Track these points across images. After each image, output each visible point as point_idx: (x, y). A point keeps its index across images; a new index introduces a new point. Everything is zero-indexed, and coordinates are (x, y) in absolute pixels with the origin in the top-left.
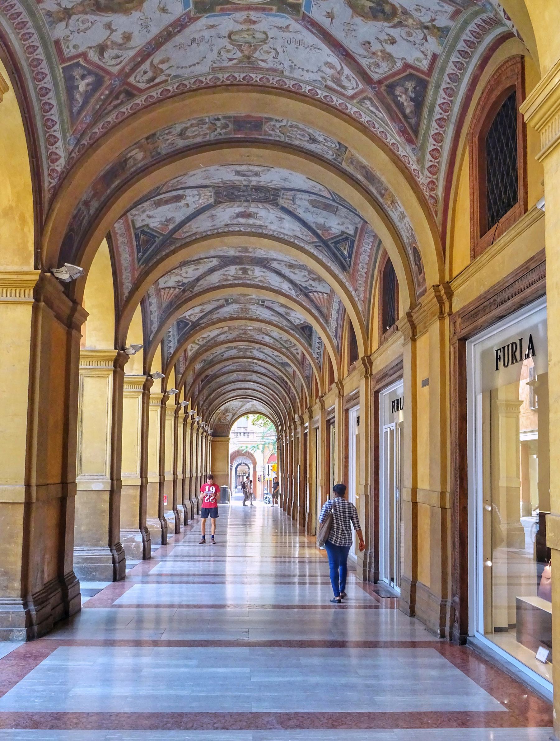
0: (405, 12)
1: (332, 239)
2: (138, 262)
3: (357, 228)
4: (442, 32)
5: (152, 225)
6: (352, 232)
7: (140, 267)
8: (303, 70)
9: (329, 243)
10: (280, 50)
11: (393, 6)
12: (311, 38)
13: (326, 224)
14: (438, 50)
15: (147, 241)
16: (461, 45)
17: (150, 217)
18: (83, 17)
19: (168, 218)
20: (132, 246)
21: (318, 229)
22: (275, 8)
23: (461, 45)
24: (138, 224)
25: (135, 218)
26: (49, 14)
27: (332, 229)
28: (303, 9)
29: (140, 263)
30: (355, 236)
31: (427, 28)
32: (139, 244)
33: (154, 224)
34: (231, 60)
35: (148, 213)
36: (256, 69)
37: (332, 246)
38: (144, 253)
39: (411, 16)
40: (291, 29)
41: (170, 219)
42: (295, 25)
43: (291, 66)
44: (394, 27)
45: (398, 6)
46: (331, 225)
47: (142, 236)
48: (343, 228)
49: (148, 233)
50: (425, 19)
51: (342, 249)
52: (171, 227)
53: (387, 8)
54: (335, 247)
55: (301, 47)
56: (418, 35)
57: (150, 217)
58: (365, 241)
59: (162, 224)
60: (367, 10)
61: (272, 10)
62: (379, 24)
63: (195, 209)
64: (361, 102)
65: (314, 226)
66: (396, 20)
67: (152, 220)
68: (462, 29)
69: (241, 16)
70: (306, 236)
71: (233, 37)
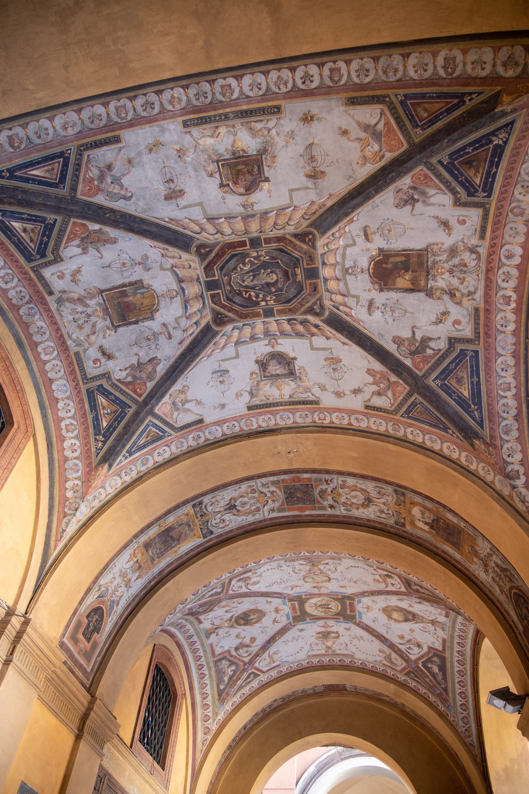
0: (232, 626)
1: (62, 232)
2: (512, 123)
3: (51, 293)
4: (208, 634)
5: (447, 199)
6: (47, 273)
7: (514, 111)
8: (272, 569)
9: (59, 219)
10: (292, 574)
11: (241, 625)
12: (276, 589)
13: (96, 253)
14: (202, 626)
15: (469, 163)
16: (195, 638)
17: (445, 224)
18: (425, 616)
19: (409, 208)
20: (511, 169)
21: (100, 231)
22: (304, 597)
23: (195, 638)
24: (474, 215)
25: (474, 241)
26: (443, 629)
27: (79, 251)
28: (287, 601)
29: (509, 119)
30: (36, 270)
31: (216, 629)
32: (490, 167)
33: (440, 201)
34: (327, 564)
35: (448, 241)
36: (306, 559)
37: (51, 217)
38: (487, 139)
39: (228, 627)
40: (290, 588)
41: (406, 202)
42: (288, 591)
43: (281, 567)
44: (232, 617)
45: (238, 627)
46: (86, 258)
47: (477, 181)
48: (67, 267)
49: (462, 184)
50: (220, 632)
51: (29, 226)
52: (406, 181)
53: (242, 622)
54: (42, 220)
55: (279, 581)
56: (217, 622)
57: (445, 224)
58: (16, 279)
59: (423, 194)
60: (251, 614)
61: (305, 595)
62: (240, 612)
63: (352, 221)
64: (223, 585)
65: (112, 232)
66: (233, 620)
67: (444, 215)
68: (203, 645)
69: (323, 591)
70: (102, 177)
71: (327, 578)
